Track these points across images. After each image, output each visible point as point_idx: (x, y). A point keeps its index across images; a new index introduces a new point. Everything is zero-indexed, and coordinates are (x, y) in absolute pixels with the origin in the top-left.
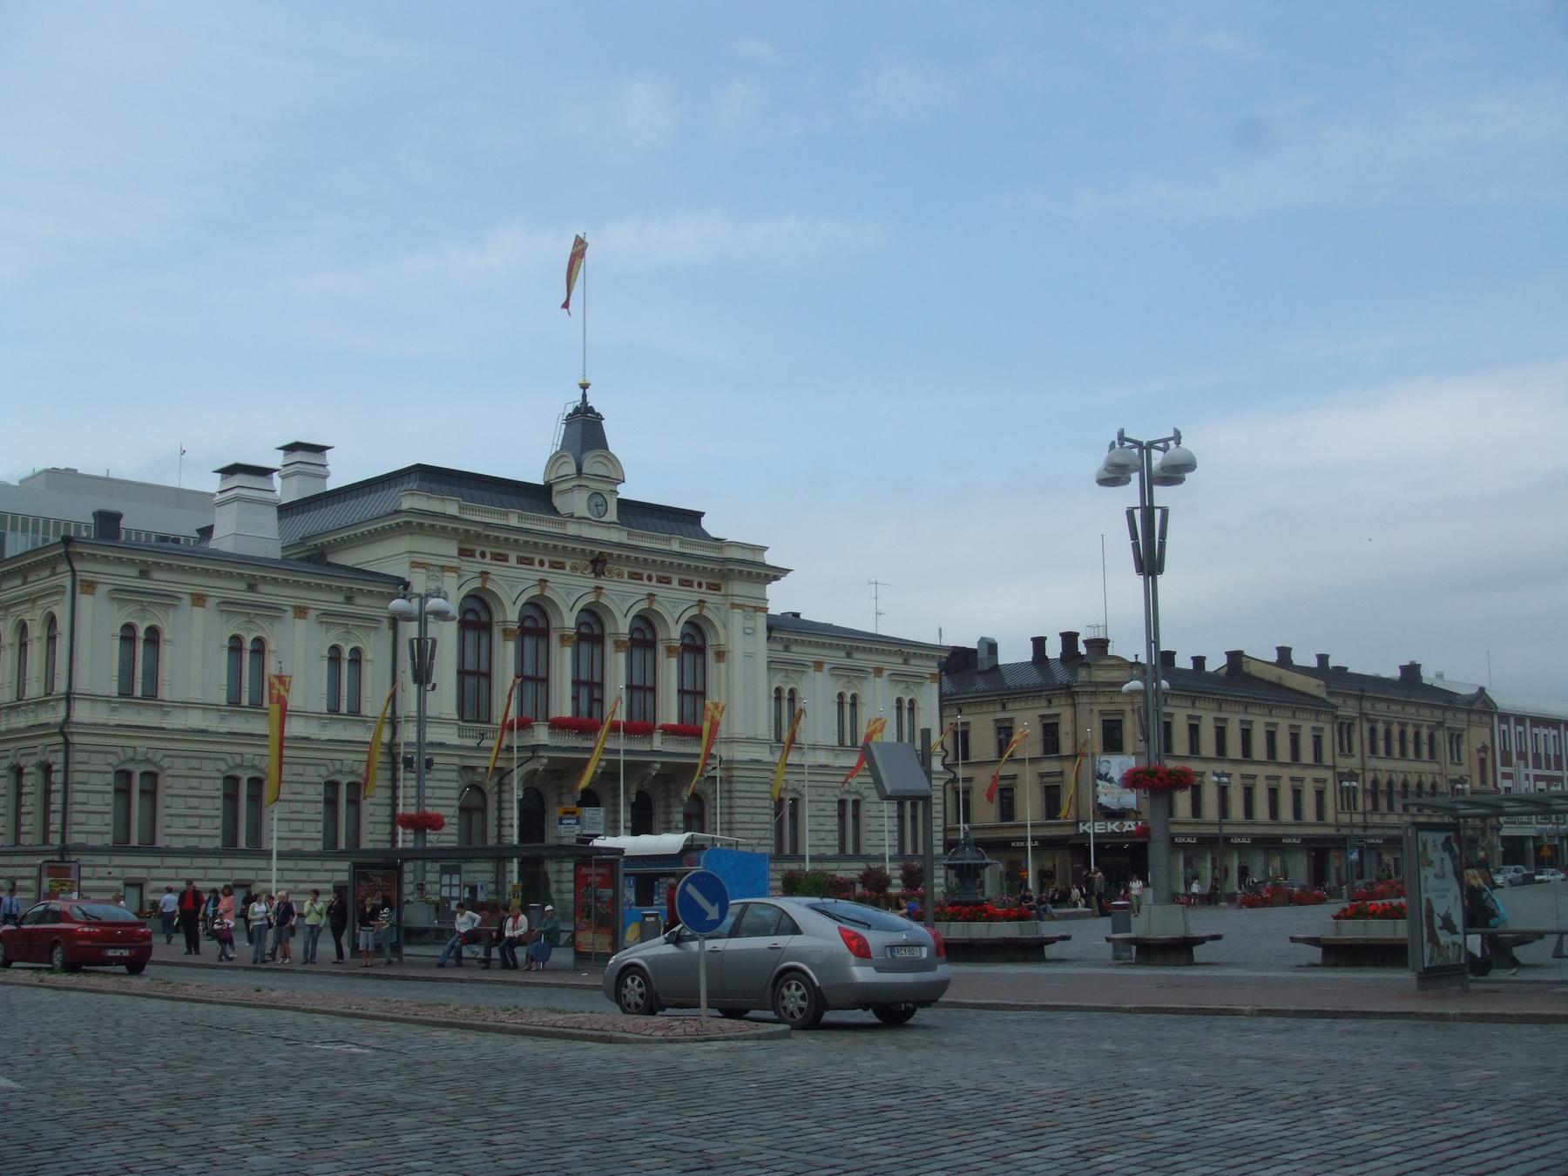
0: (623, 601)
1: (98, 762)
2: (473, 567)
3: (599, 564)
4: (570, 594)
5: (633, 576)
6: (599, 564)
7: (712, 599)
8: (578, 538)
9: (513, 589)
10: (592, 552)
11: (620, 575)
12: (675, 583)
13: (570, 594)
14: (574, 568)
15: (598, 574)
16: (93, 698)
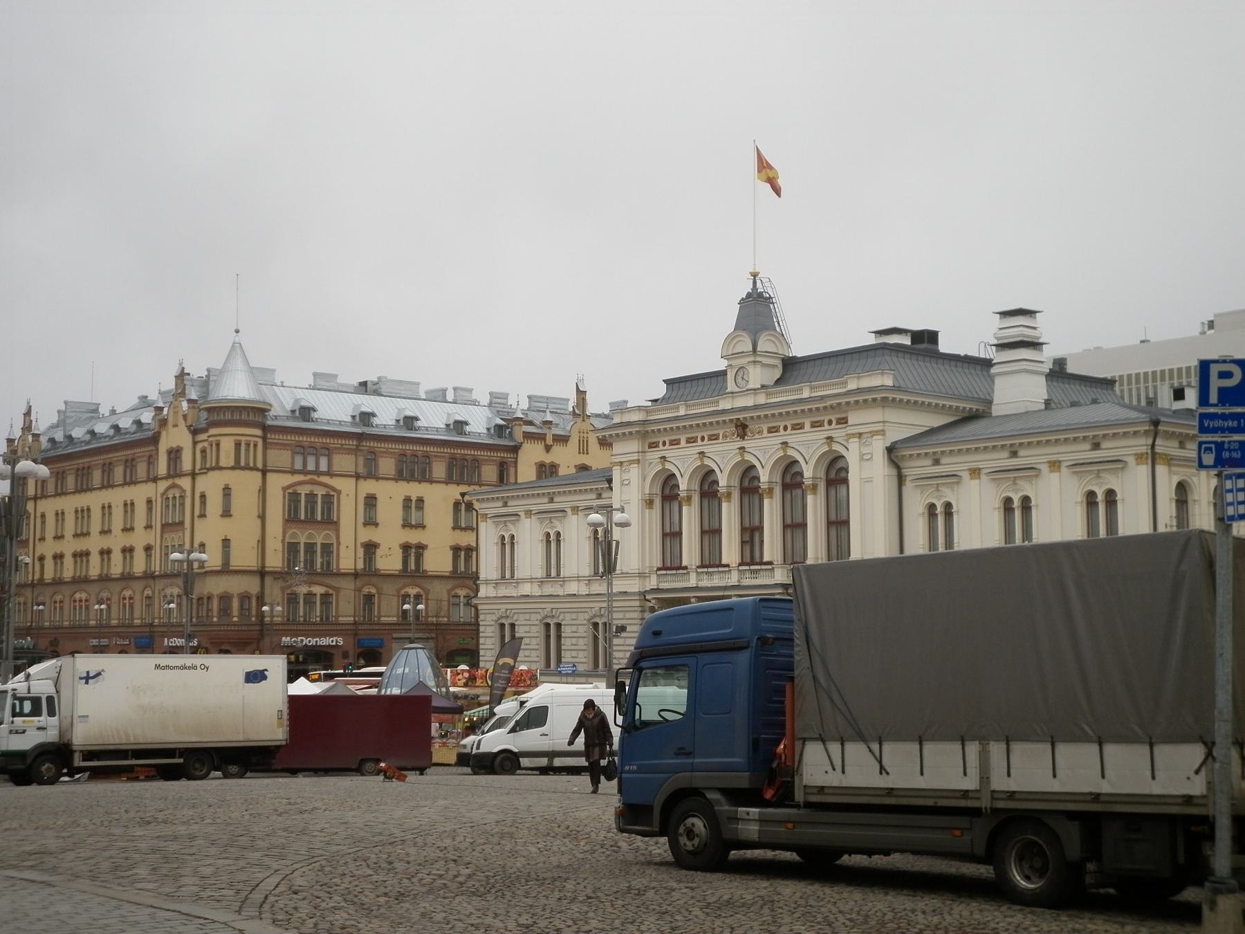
0: (764, 453)
1: (489, 617)
2: (654, 455)
3: (742, 429)
4: (724, 458)
5: (771, 430)
6: (742, 429)
7: (838, 433)
8: (724, 412)
9: (684, 462)
10: (731, 421)
11: (760, 432)
12: (807, 427)
13: (724, 458)
14: (725, 437)
15: (742, 436)
16: (487, 582)
